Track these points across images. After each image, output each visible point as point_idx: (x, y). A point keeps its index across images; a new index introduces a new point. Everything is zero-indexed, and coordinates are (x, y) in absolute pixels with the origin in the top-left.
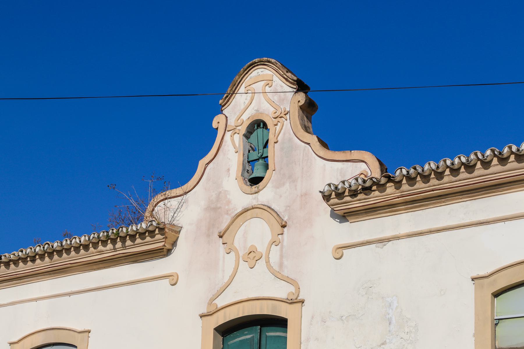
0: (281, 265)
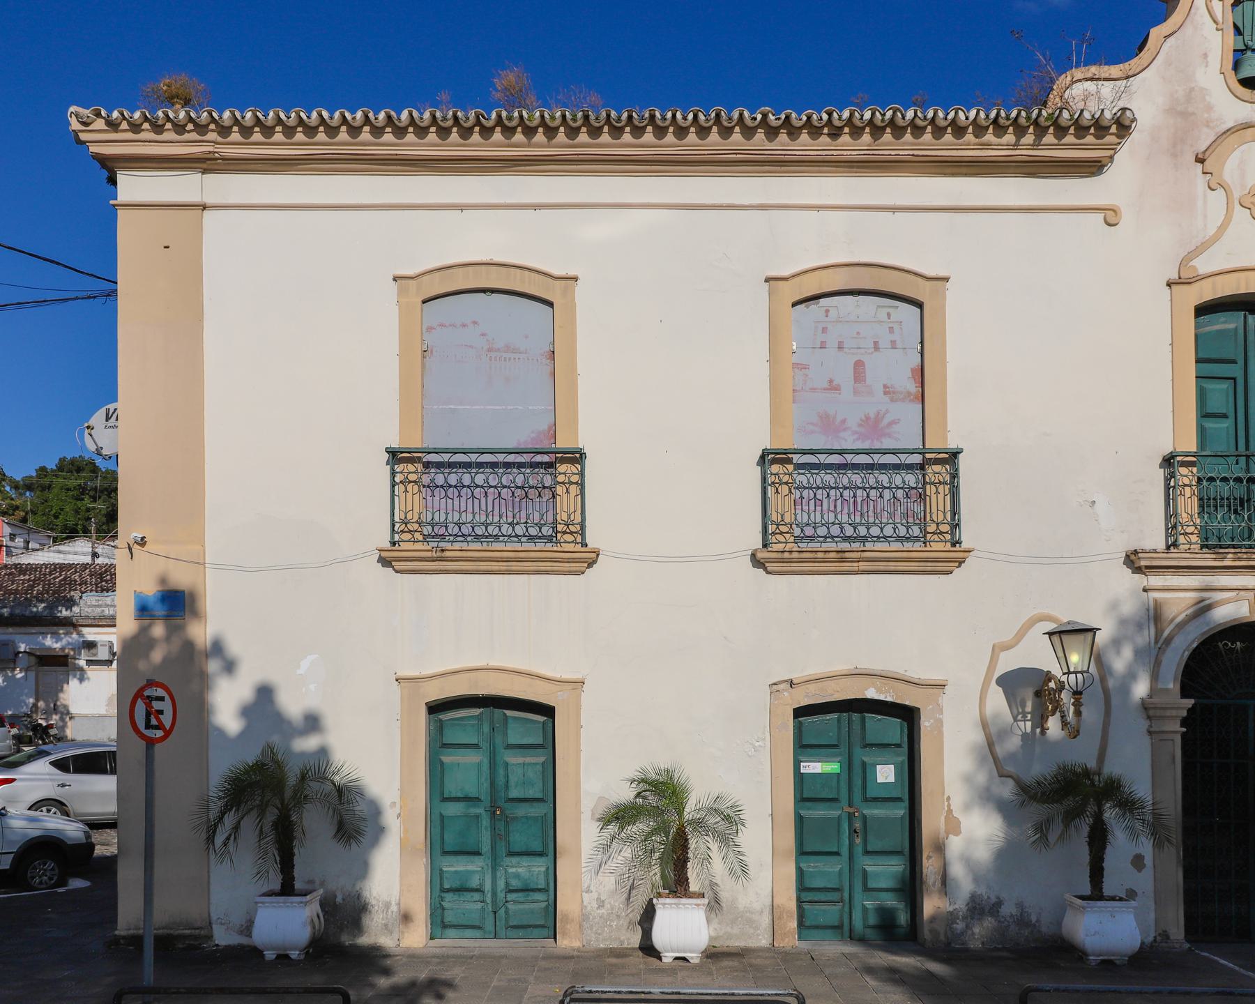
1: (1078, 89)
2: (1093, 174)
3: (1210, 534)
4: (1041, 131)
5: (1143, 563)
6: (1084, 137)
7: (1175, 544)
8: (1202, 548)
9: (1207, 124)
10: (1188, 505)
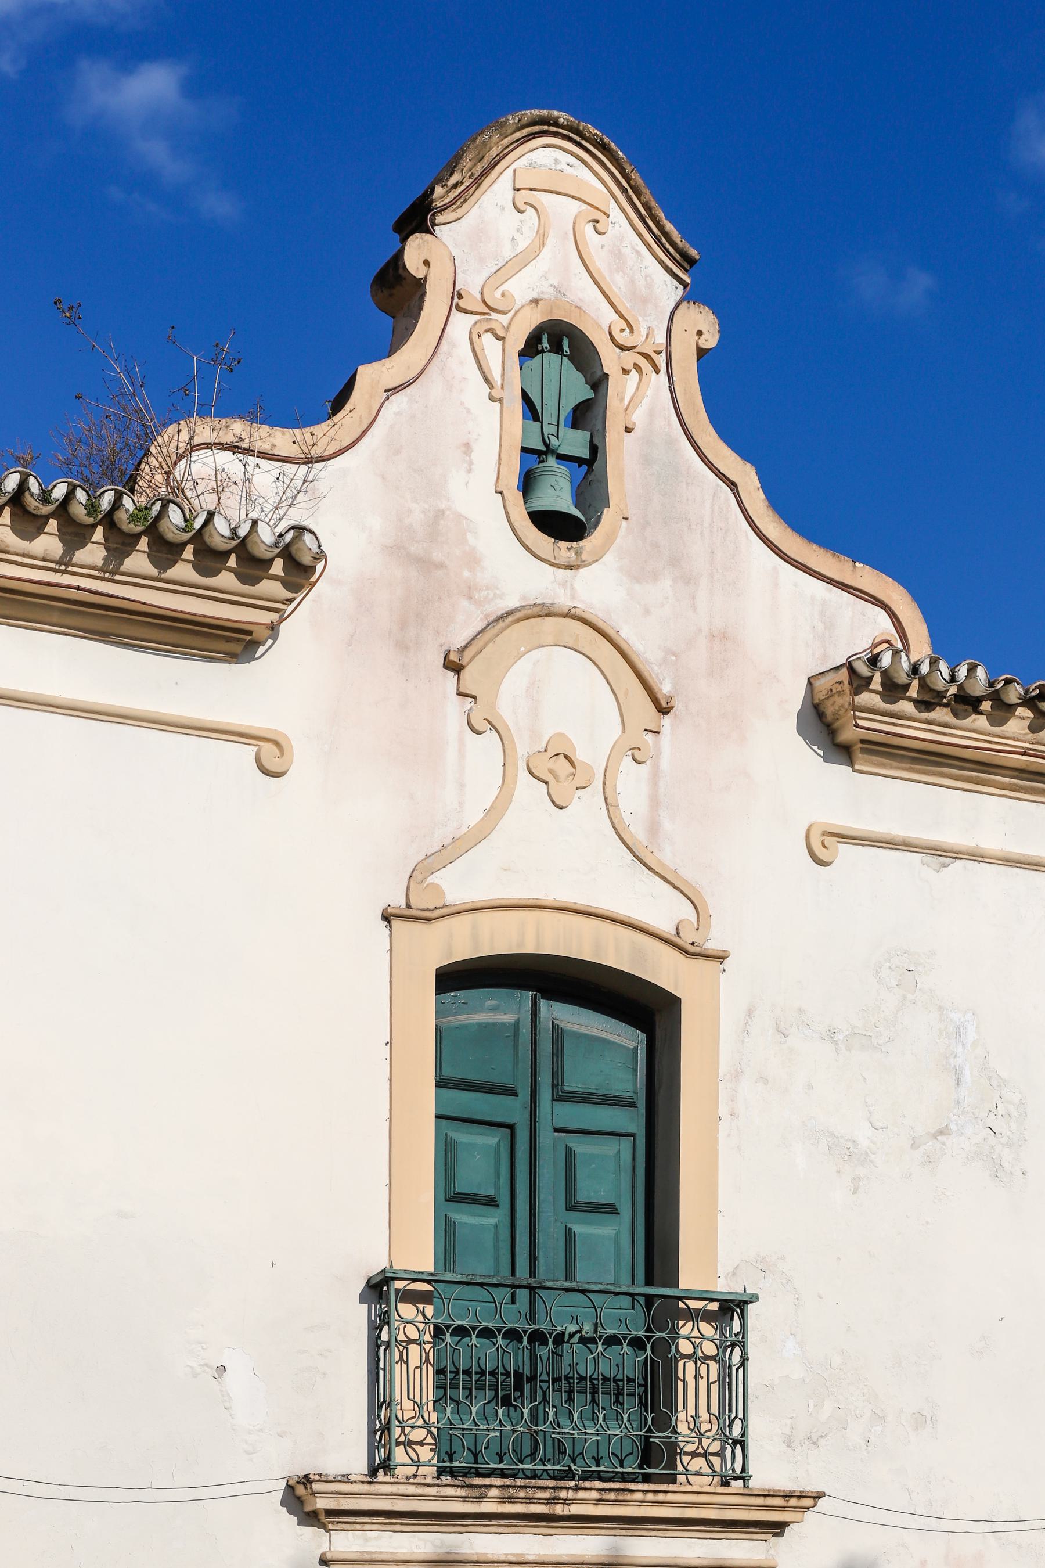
0: (654, 828)
1: (204, 465)
2: (233, 657)
3: (456, 1446)
4: (120, 544)
5: (322, 1504)
6: (215, 573)
7: (386, 1466)
8: (441, 1472)
9: (469, 592)
10: (414, 1382)
